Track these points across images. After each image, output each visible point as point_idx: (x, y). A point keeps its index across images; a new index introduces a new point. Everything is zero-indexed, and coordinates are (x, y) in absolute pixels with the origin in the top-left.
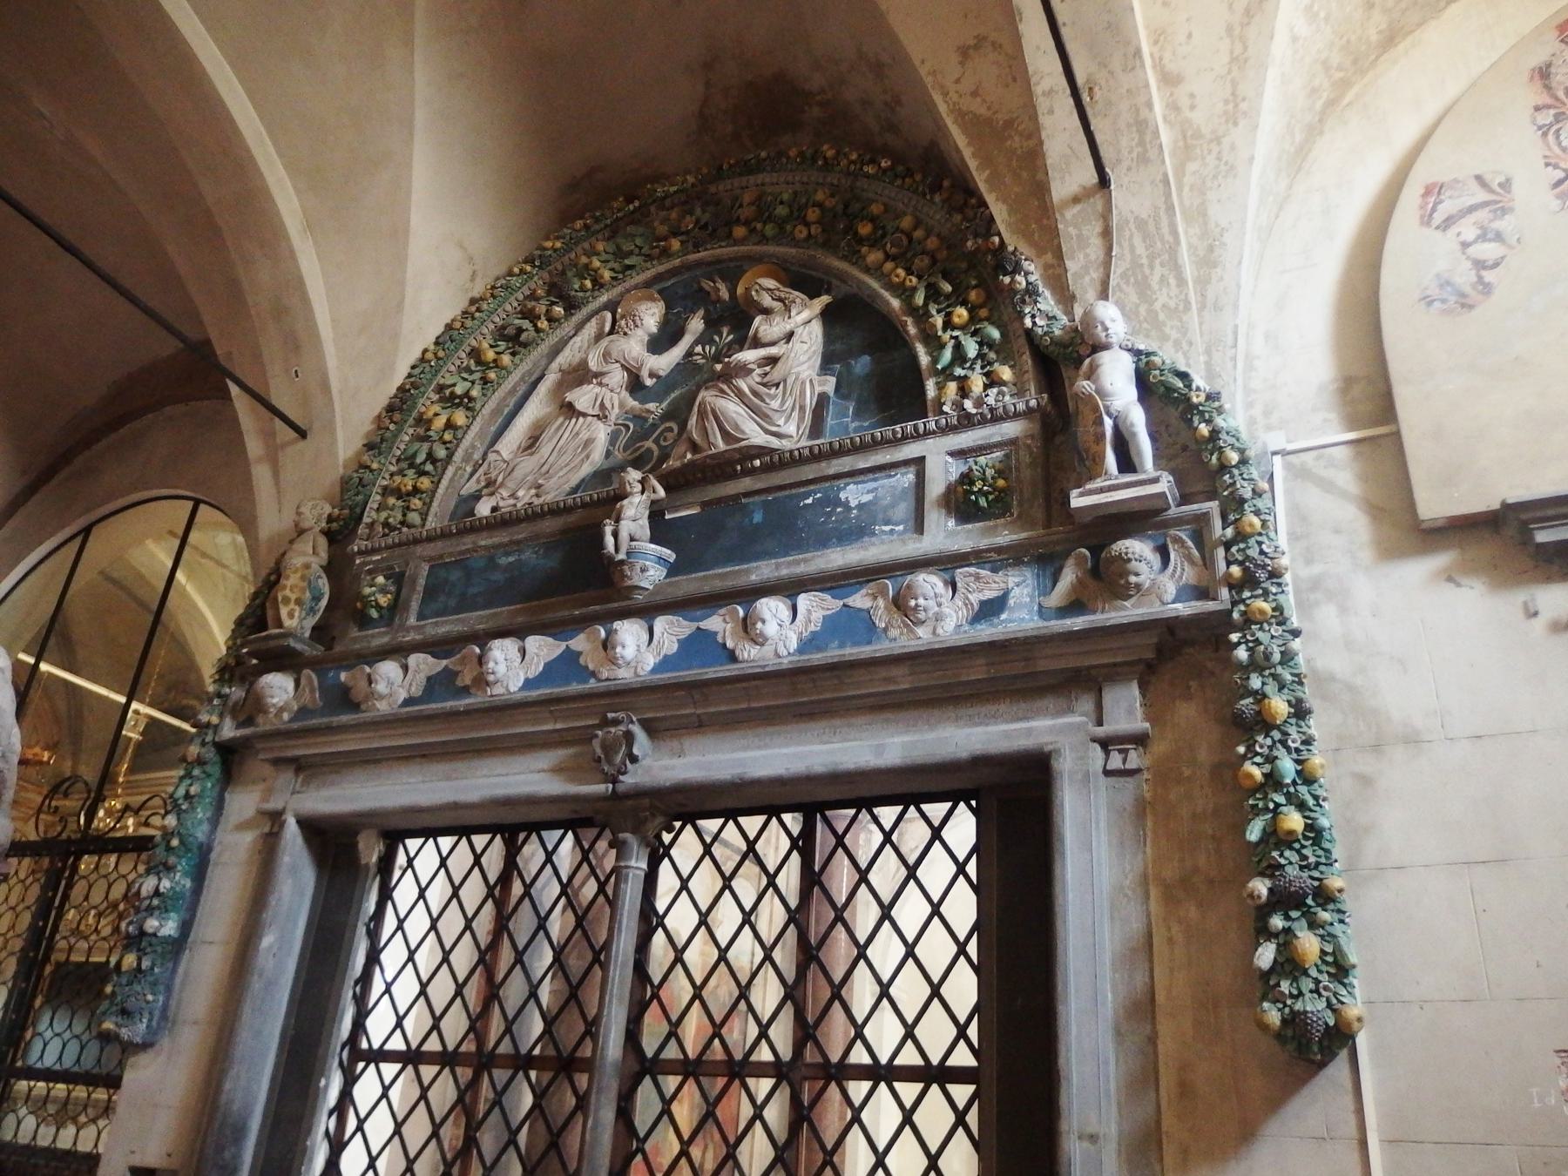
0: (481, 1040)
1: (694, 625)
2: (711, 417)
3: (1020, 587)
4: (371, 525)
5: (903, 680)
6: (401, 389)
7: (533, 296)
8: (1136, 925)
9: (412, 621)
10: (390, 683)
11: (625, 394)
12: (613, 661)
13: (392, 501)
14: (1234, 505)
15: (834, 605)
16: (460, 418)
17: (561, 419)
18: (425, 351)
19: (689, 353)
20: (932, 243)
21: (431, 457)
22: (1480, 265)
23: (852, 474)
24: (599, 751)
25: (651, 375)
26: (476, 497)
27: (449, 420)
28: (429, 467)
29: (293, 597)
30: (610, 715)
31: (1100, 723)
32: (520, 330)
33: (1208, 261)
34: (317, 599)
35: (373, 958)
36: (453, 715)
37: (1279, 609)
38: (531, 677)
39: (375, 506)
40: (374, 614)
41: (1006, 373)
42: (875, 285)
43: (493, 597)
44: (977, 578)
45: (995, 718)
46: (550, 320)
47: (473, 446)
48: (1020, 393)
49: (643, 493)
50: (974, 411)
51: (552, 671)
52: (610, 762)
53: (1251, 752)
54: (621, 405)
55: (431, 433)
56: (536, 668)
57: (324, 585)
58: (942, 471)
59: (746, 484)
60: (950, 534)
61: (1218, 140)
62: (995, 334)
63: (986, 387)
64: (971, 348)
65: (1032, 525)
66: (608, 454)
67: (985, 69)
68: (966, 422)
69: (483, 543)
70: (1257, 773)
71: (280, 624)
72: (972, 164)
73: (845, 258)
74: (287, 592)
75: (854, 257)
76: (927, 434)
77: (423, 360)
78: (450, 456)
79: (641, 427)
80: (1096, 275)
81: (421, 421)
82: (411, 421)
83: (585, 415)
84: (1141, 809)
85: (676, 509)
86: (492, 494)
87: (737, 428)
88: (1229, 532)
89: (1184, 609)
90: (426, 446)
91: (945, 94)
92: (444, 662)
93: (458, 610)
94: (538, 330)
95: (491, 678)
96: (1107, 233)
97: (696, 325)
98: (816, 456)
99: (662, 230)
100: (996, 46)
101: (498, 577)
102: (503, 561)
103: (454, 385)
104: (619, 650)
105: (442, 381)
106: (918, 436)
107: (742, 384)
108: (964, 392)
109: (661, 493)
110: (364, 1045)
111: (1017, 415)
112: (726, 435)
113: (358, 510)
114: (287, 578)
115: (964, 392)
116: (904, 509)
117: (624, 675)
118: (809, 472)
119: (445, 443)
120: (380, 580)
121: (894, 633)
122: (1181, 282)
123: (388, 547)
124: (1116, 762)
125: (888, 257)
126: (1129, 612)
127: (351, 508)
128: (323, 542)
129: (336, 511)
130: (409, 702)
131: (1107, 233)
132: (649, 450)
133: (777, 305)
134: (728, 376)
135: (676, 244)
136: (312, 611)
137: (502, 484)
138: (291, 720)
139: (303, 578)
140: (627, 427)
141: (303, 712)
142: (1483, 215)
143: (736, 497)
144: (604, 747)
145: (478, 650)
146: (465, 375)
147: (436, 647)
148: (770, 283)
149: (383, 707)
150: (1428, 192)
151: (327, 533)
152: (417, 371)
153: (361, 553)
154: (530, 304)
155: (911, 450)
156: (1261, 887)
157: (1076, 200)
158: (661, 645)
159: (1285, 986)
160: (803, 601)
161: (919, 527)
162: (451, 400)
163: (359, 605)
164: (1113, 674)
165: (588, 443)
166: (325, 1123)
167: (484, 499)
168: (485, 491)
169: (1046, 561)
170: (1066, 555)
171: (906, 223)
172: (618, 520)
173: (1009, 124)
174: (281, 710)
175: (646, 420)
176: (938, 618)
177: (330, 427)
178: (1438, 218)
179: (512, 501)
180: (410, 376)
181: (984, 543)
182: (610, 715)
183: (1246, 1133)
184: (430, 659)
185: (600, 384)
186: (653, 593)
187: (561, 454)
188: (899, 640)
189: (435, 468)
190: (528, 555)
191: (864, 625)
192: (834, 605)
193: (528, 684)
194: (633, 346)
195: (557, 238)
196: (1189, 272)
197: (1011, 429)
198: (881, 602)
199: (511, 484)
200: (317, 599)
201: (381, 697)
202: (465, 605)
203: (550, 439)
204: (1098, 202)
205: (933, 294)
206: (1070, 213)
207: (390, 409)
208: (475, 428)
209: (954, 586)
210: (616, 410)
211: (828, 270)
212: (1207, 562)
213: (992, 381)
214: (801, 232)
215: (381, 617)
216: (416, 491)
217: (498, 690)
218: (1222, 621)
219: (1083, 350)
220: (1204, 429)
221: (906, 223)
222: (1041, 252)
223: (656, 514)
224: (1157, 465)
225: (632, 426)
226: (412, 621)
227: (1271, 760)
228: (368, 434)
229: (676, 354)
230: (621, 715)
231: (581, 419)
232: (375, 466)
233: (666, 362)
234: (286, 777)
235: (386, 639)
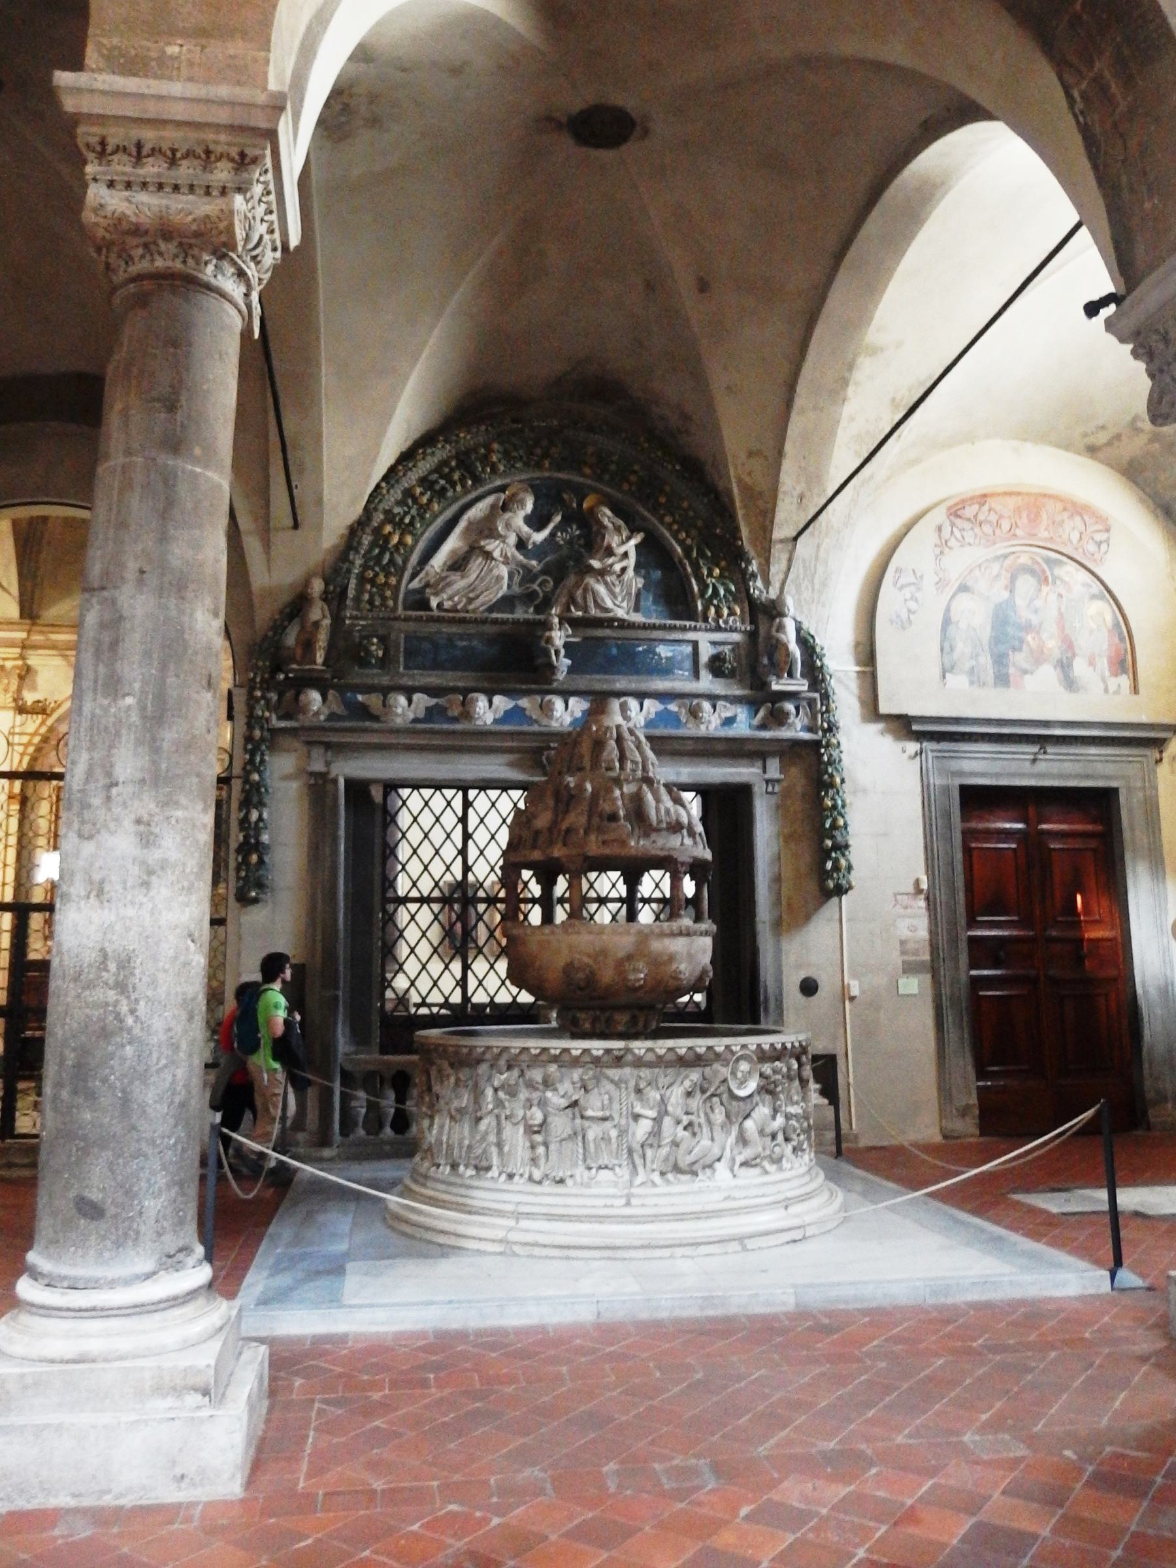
3: (741, 713)
4: (357, 599)
5: (690, 746)
6: (366, 508)
7: (444, 463)
8: (776, 849)
9: (401, 669)
11: (514, 550)
13: (368, 587)
14: (826, 697)
15: (660, 707)
16: (409, 540)
18: (378, 486)
19: (553, 535)
20: (700, 523)
22: (909, 611)
23: (662, 641)
25: (534, 543)
27: (400, 539)
31: (765, 772)
32: (444, 489)
33: (824, 584)
37: (839, 743)
38: (497, 716)
40: (373, 661)
41: (738, 610)
42: (667, 534)
43: (455, 664)
44: (725, 707)
45: (723, 765)
46: (464, 486)
48: (743, 622)
50: (723, 626)
51: (509, 716)
53: (827, 794)
56: (500, 714)
58: (706, 652)
59: (607, 632)
60: (711, 682)
61: (839, 532)
62: (733, 588)
63: (729, 615)
64: (722, 592)
65: (744, 688)
66: (509, 586)
67: (756, 465)
68: (718, 629)
70: (830, 803)
72: (738, 504)
73: (649, 511)
75: (654, 510)
76: (700, 630)
78: (405, 561)
79: (528, 576)
80: (781, 576)
84: (778, 807)
87: (603, 600)
88: (824, 708)
89: (806, 736)
91: (736, 468)
94: (455, 490)
96: (790, 560)
97: (558, 519)
98: (644, 627)
99: (538, 451)
100: (766, 458)
101: (458, 653)
106: (695, 629)
107: (608, 579)
108: (719, 614)
109: (570, 632)
111: (740, 631)
112: (595, 601)
115: (719, 614)
116: (688, 664)
117: (555, 725)
118: (642, 634)
119: (399, 554)
121: (690, 725)
122: (813, 590)
123: (373, 618)
124: (770, 789)
125: (674, 522)
126: (785, 733)
128: (326, 607)
130: (416, 720)
131: (790, 560)
132: (535, 591)
133: (610, 525)
134: (602, 573)
135: (547, 463)
137: (443, 590)
138: (326, 720)
141: (332, 717)
142: (913, 588)
143: (603, 639)
148: (608, 512)
149: (399, 721)
150: (896, 571)
153: (351, 618)
154: (446, 470)
155: (691, 636)
156: (829, 843)
157: (782, 541)
158: (572, 712)
159: (835, 875)
160: (647, 702)
161: (696, 675)
162: (398, 524)
164: (773, 754)
168: (428, 590)
169: (753, 704)
170: (763, 703)
171: (685, 504)
173: (760, 493)
174: (317, 713)
176: (709, 722)
177: (319, 527)
178: (899, 585)
179: (450, 603)
180: (368, 501)
181: (729, 693)
183: (808, 918)
185: (504, 542)
187: (482, 580)
188: (690, 730)
190: (475, 643)
191: (674, 719)
192: (660, 707)
193: (496, 721)
194: (518, 519)
195: (469, 432)
196: (817, 586)
197: (736, 637)
198: (683, 711)
199: (450, 591)
201: (397, 715)
202: (437, 665)
204: (790, 546)
205: (701, 554)
206: (779, 546)
209: (714, 707)
211: (638, 512)
212: (814, 717)
213: (732, 613)
214: (626, 487)
217: (479, 722)
218: (817, 744)
219: (774, 612)
220: (818, 663)
221: (685, 504)
222: (759, 556)
224: (802, 675)
226: (401, 669)
227: (833, 799)
228: (342, 536)
229: (545, 533)
233: (539, 537)
234: (317, 753)
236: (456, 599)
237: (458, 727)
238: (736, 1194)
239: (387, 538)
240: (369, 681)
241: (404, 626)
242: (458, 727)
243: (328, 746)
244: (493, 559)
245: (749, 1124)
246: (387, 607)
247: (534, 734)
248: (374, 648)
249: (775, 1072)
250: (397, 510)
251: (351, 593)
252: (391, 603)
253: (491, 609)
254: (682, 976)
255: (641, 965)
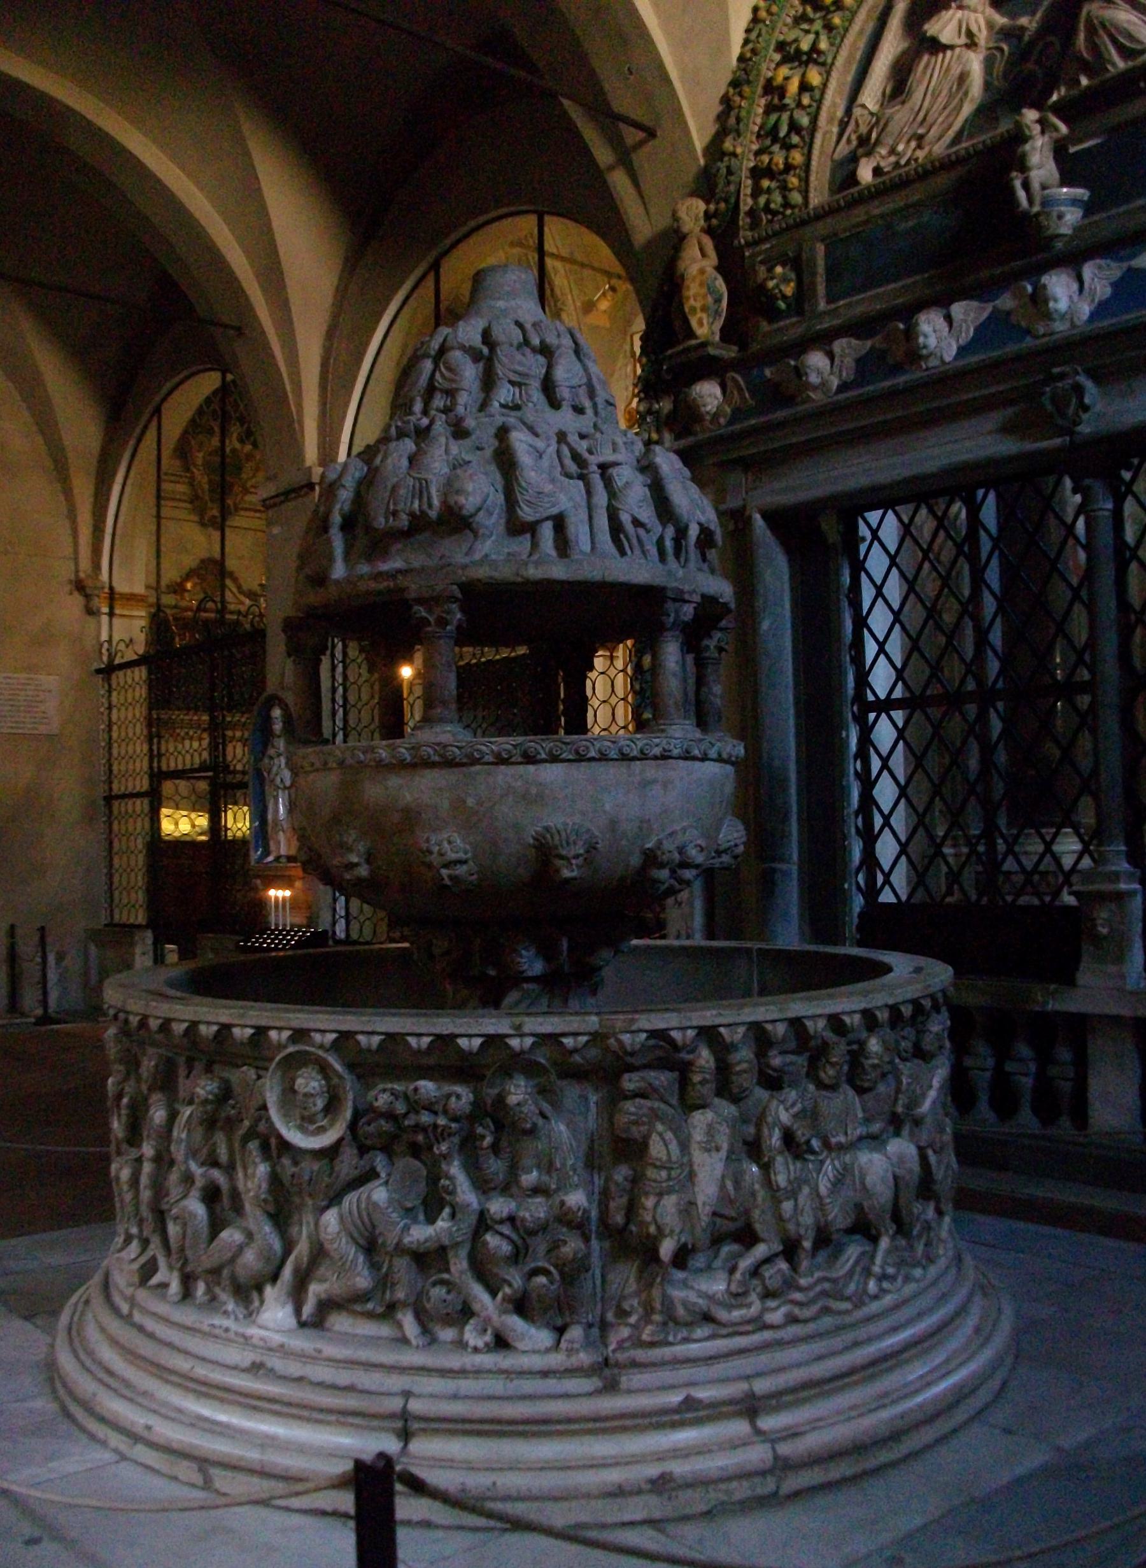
0: (980, 682)
1: (1125, 265)
2: (1101, 32)
4: (751, 213)
6: (741, 59)
9: (822, 305)
10: (819, 372)
11: (990, 11)
12: (1048, 316)
13: (766, 183)
16: (815, 77)
17: (926, 58)
21: (794, 127)
24: (1049, 407)
26: (853, 159)
28: (795, 139)
29: (698, 305)
30: (1056, 370)
34: (718, 301)
35: (861, 622)
36: (892, 394)
39: (749, 191)
40: (782, 305)
47: (834, 104)
49: (1043, 132)
51: (984, 334)
52: (1063, 415)
54: (990, 25)
55: (787, 101)
56: (968, 333)
57: (721, 284)
66: (987, 85)
69: (876, 212)
71: (691, 334)
74: (692, 302)
77: (755, 20)
78: (814, 120)
81: (770, 88)
82: (760, 90)
83: (952, 47)
85: (1081, 141)
86: (868, 154)
87: (1130, 37)
90: (785, 116)
92: (869, 343)
93: (865, 288)
95: (924, 352)
102: (903, 226)
103: (796, 40)
104: (1051, 304)
105: (781, 38)
109: (1063, 129)
110: (871, 698)
113: (733, 200)
114: (688, 288)
120: (779, 270)
123: (775, 234)
127: (726, 201)
129: (712, 207)
130: (843, 387)
136: (717, 313)
137: (878, 142)
139: (701, 285)
140: (1001, 50)
141: (738, 414)
144: (1053, 400)
145: (901, 326)
146: (805, 26)
147: (857, 329)
151: (709, 231)
152: (753, 36)
153: (748, 244)
158: (1093, 292)
163: (763, 299)
165: (963, 78)
166: (854, 766)
167: (863, 161)
172: (1024, 168)
174: (716, 416)
175: (1020, 38)
179: (893, 159)
180: (746, 42)
182: (1056, 370)
184: (854, 342)
186: (1072, 238)
187: (935, 97)
189: (802, 138)
193: (962, 351)
200: (718, 301)
201: (815, 388)
203: (920, 82)
207: (735, 84)
208: (833, 84)
210: (984, 32)
215: (789, 306)
216: (789, 167)
217: (933, 362)
223: (1059, 151)
225: (1006, 48)
226: (822, 305)
230: (1066, 369)
231: (949, 53)
232: (739, 150)
234: (736, 478)
235: (800, 330)
236: (900, 148)
237: (901, 380)
238: (276, 1363)
239: (782, 91)
240: (776, 340)
241: (822, 228)
242: (901, 380)
243: (747, 464)
244: (945, 48)
245: (331, 1218)
246: (793, 207)
247: (1034, 353)
248: (771, 284)
249: (415, 1105)
250: (791, 36)
251: (746, 203)
252: (796, 198)
253: (957, 140)
254: (435, 859)
255: (351, 837)
